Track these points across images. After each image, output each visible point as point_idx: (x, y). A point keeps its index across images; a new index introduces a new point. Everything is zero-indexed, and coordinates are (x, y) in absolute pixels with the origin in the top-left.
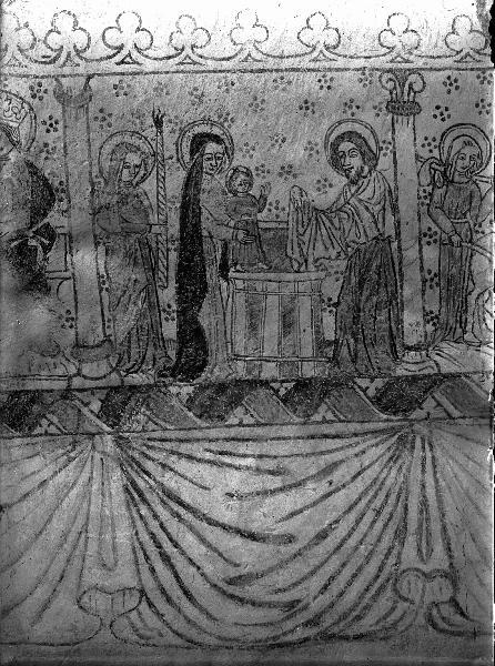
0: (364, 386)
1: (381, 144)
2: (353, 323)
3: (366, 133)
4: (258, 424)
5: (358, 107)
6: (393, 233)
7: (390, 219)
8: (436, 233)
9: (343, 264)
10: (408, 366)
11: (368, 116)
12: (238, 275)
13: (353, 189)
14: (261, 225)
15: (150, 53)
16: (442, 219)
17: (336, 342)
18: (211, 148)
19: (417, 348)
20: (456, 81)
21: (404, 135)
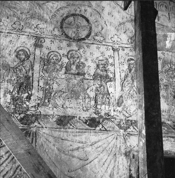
0: (17, 116)
1: (31, 53)
3: (27, 50)
6: (31, 75)
7: (31, 72)
8: (44, 77)
20: (53, 41)
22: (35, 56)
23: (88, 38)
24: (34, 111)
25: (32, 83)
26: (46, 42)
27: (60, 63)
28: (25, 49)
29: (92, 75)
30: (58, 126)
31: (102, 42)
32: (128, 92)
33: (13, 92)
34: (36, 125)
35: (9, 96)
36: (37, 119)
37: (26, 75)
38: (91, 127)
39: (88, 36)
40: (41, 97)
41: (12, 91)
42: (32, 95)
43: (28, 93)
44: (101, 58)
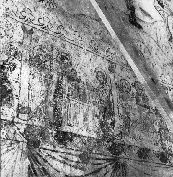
0: (106, 144)
3: (104, 73)
6: (112, 100)
7: (111, 97)
8: (121, 104)
12: (72, 99)
22: (111, 81)
24: (119, 140)
25: (114, 109)
26: (117, 68)
27: (131, 92)
30: (141, 160)
33: (99, 116)
34: (123, 156)
35: (97, 120)
37: (108, 99)
38: (162, 162)
40: (122, 126)
41: (98, 115)
42: (115, 123)
43: (112, 120)
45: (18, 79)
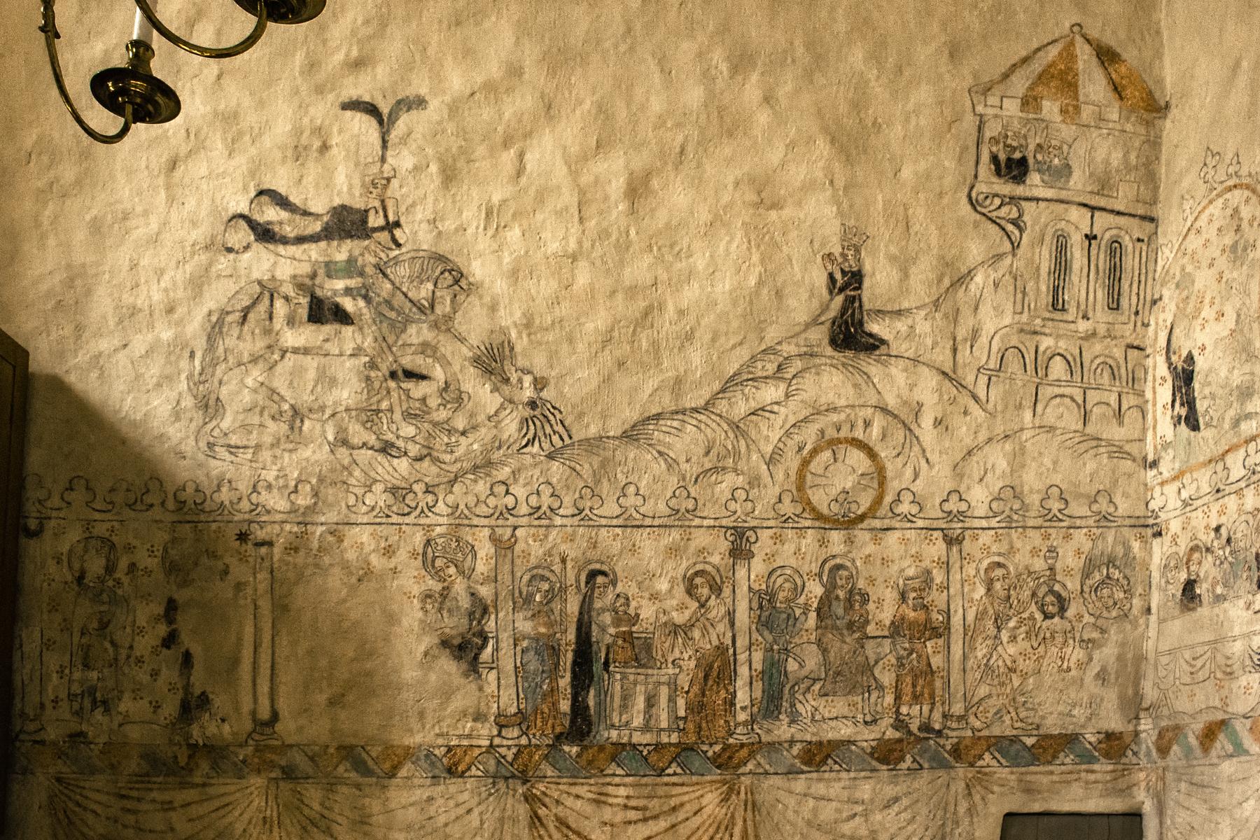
2: (698, 707)
3: (714, 572)
4: (627, 775)
5: (708, 553)
6: (730, 642)
9: (693, 664)
10: (741, 736)
11: (716, 559)
13: (703, 611)
14: (635, 635)
15: (561, 511)
16: (766, 633)
17: (685, 718)
18: (600, 580)
19: (745, 724)
21: (741, 573)
23: (876, 511)
27: (802, 600)
28: (709, 568)
29: (888, 623)
31: (914, 519)
32: (985, 661)
36: (752, 755)
39: (878, 501)
44: (911, 572)
45: (493, 662)
